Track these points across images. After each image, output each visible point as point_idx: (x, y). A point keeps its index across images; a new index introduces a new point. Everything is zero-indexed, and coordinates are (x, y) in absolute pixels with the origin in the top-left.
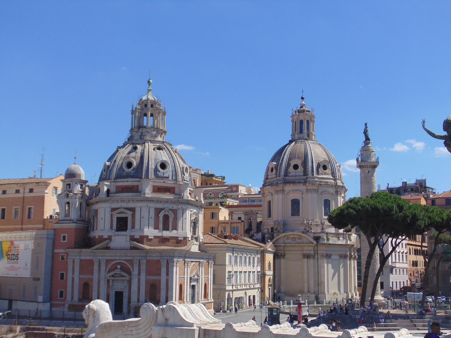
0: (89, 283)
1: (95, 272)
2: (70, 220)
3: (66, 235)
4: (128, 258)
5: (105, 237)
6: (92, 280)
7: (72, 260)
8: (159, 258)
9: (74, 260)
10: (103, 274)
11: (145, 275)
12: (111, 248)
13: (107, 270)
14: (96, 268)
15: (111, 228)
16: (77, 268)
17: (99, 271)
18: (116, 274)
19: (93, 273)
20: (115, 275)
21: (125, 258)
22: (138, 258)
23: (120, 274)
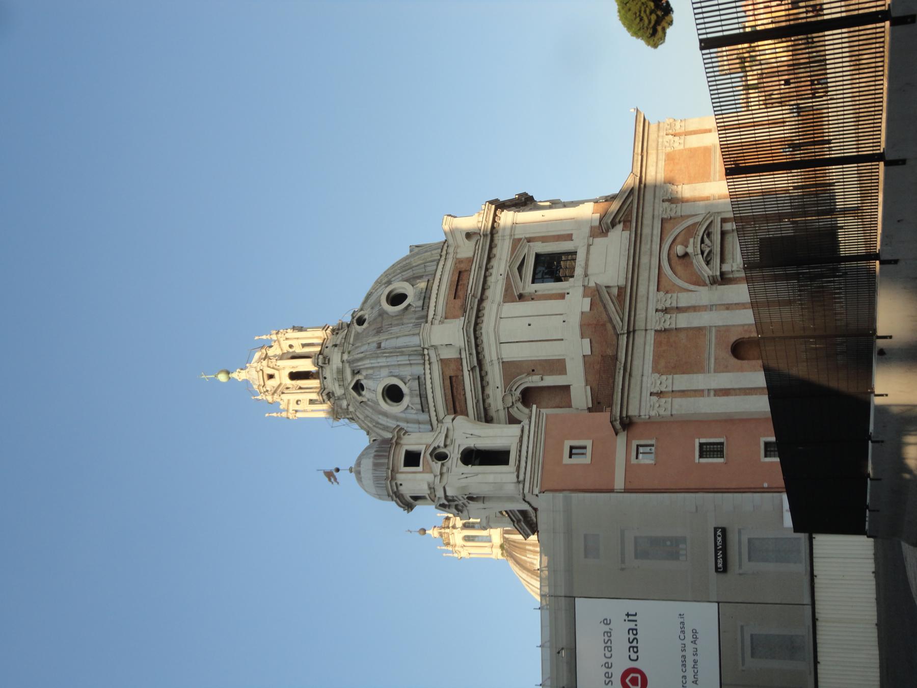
0: (733, 339)
1: (696, 323)
2: (521, 441)
3: (568, 444)
4: (657, 231)
5: (587, 308)
6: (723, 331)
7: (655, 398)
8: (662, 157)
9: (651, 394)
10: (704, 295)
11: (707, 184)
12: (622, 282)
13: (692, 287)
14: (682, 321)
15: (562, 296)
16: (682, 382)
17: (694, 309)
18: (702, 253)
19: (699, 329)
20: (705, 254)
21: (657, 239)
22: (657, 206)
23: (702, 242)
